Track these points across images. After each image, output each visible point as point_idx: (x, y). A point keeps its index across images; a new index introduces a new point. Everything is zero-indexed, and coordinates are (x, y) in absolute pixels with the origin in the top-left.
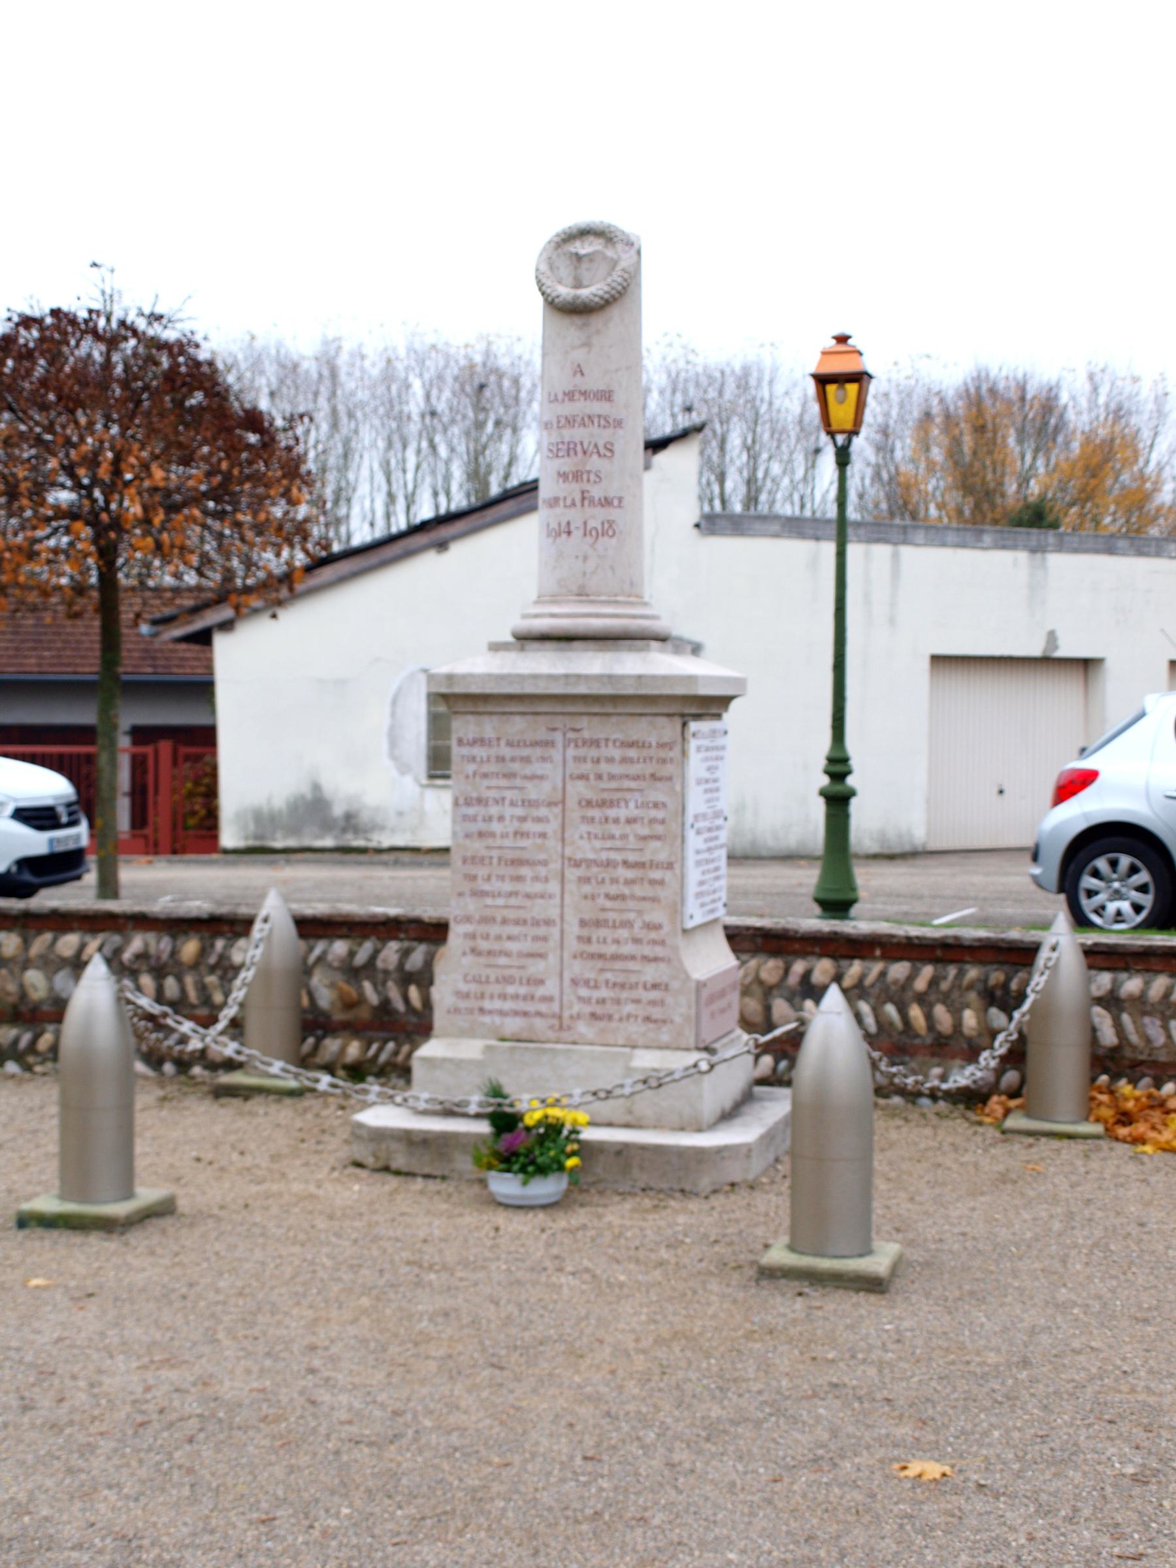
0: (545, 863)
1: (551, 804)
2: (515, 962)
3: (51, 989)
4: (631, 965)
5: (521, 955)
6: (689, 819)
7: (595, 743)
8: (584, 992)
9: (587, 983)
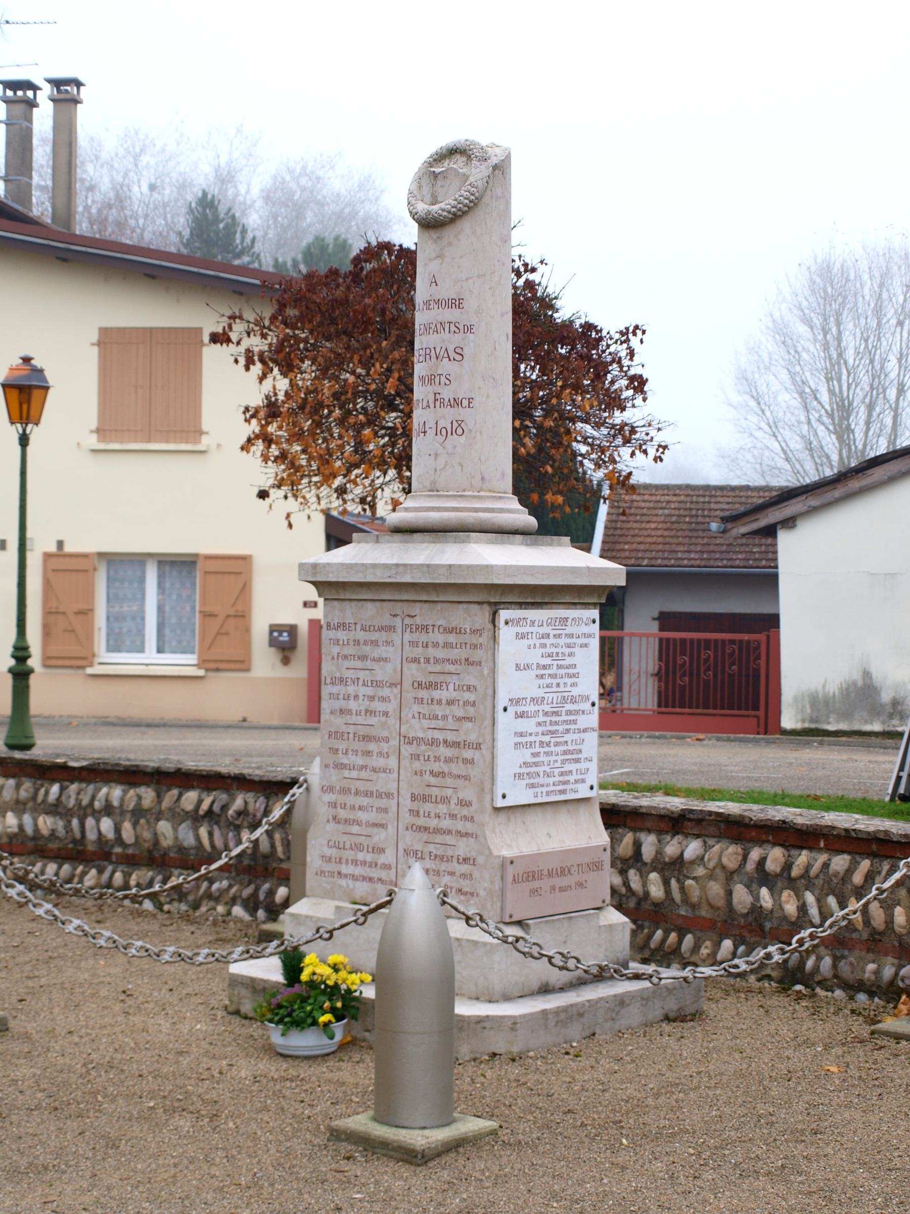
0: (387, 740)
1: (392, 685)
3: (176, 838)
4: (449, 839)
6: (502, 701)
7: (425, 628)
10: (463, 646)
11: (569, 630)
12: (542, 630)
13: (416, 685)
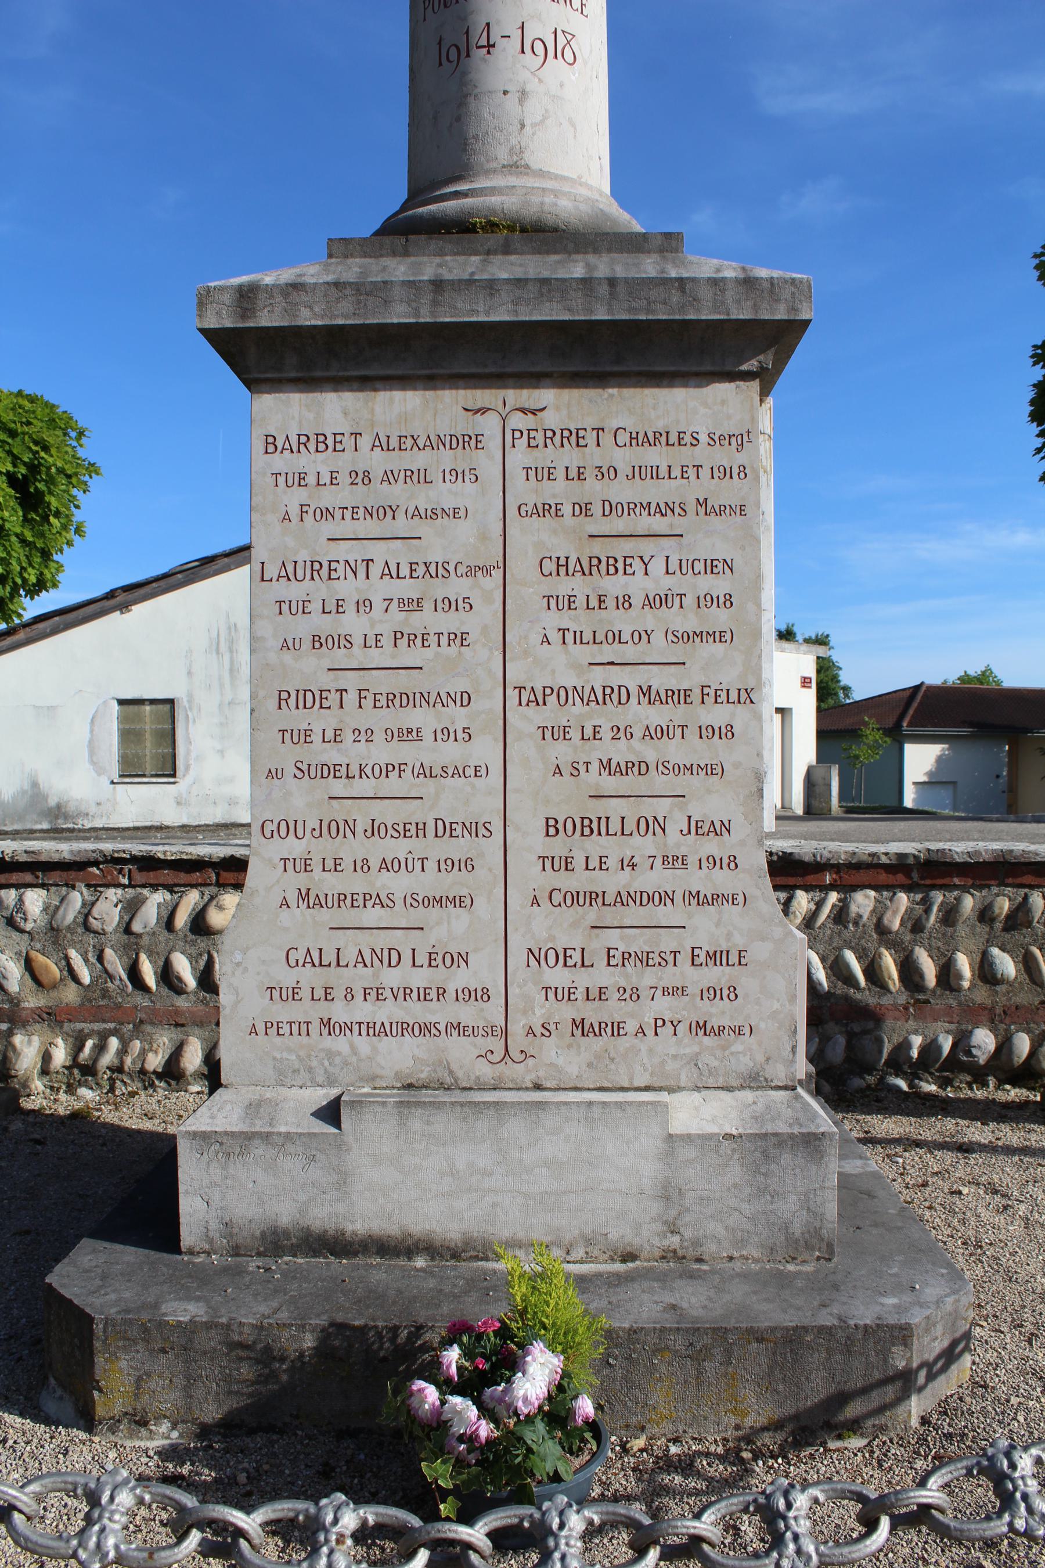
0: (465, 699)
2: (400, 916)
4: (663, 914)
5: (413, 901)
7: (574, 437)
8: (558, 976)
9: (563, 957)
10: (691, 472)
13: (549, 566)
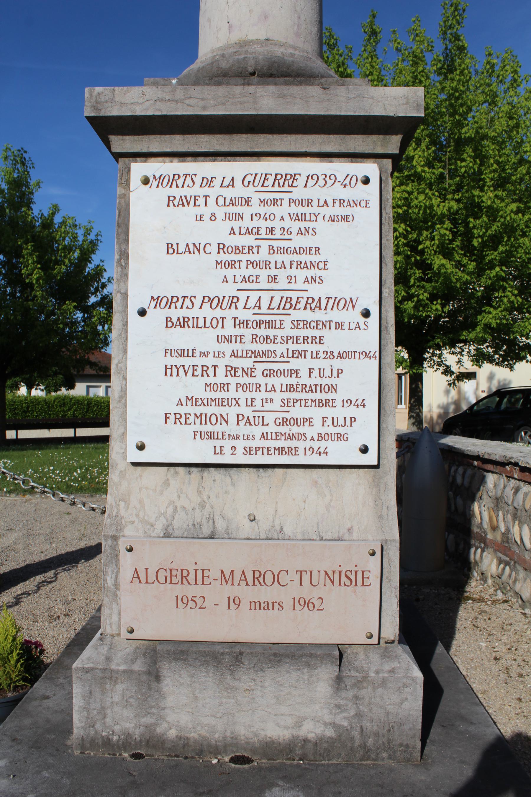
11: (298, 193)
12: (229, 193)
